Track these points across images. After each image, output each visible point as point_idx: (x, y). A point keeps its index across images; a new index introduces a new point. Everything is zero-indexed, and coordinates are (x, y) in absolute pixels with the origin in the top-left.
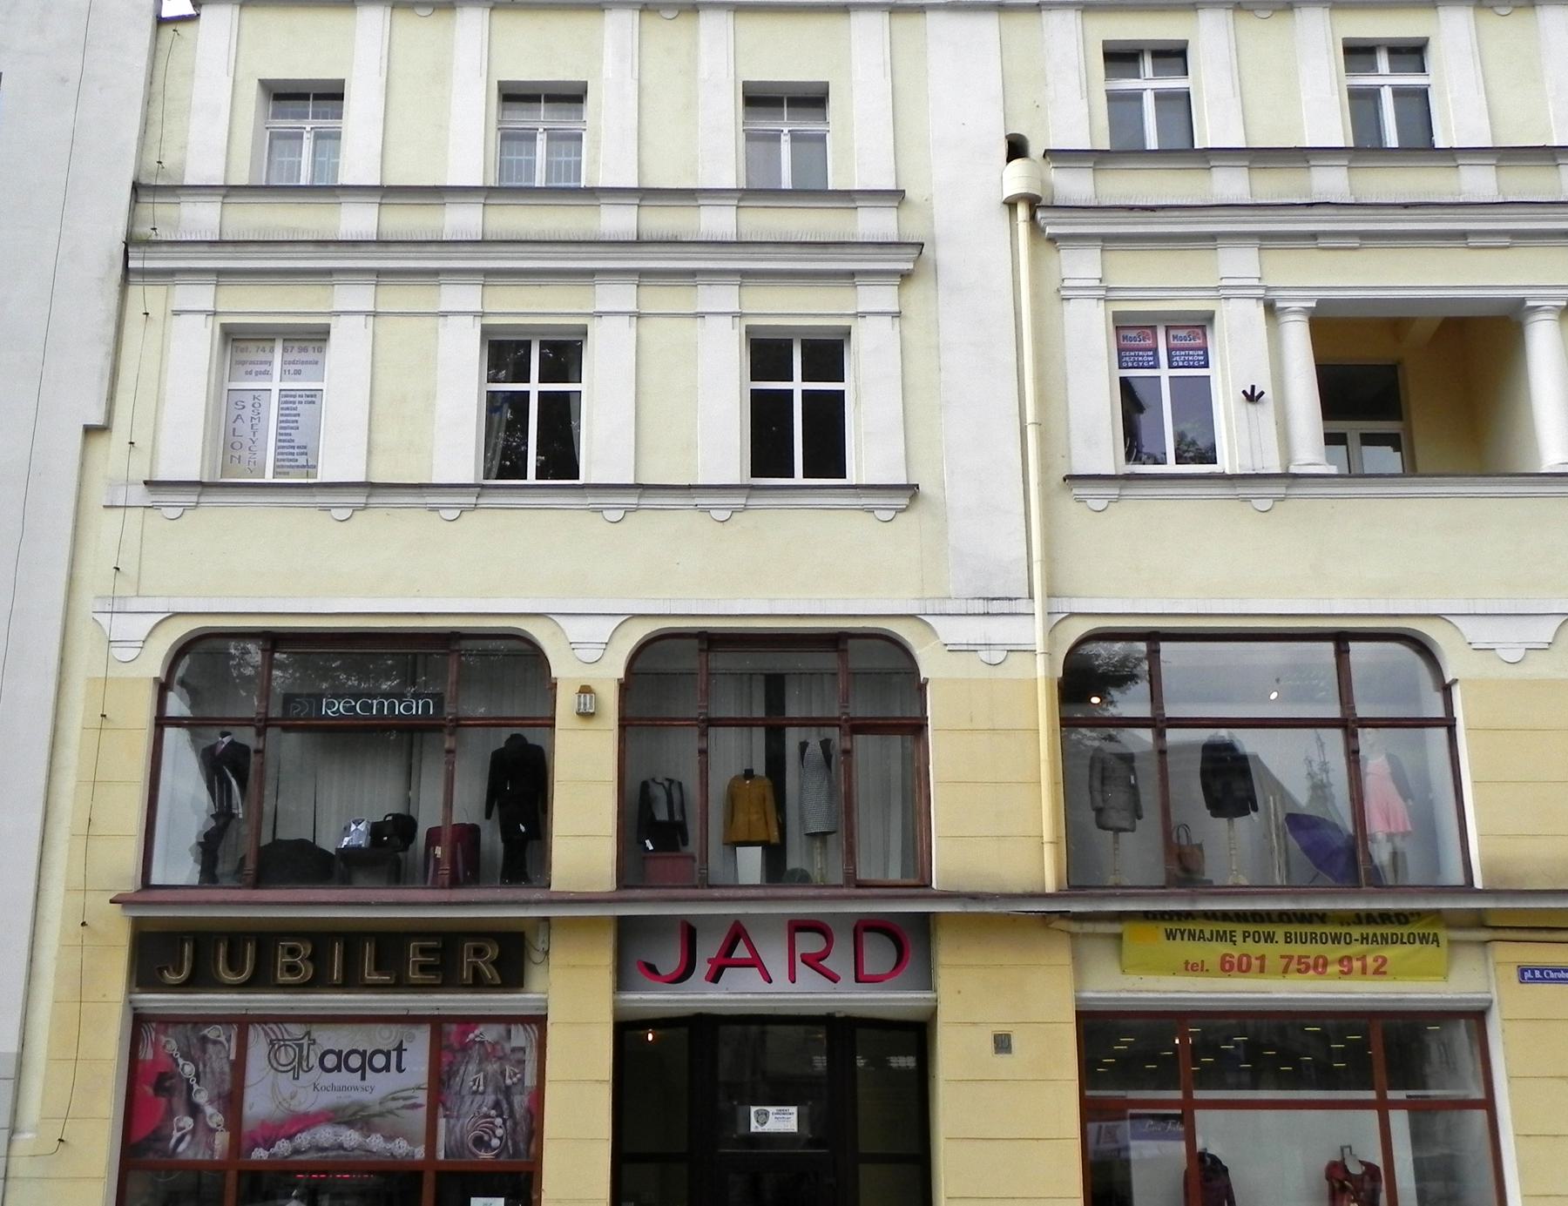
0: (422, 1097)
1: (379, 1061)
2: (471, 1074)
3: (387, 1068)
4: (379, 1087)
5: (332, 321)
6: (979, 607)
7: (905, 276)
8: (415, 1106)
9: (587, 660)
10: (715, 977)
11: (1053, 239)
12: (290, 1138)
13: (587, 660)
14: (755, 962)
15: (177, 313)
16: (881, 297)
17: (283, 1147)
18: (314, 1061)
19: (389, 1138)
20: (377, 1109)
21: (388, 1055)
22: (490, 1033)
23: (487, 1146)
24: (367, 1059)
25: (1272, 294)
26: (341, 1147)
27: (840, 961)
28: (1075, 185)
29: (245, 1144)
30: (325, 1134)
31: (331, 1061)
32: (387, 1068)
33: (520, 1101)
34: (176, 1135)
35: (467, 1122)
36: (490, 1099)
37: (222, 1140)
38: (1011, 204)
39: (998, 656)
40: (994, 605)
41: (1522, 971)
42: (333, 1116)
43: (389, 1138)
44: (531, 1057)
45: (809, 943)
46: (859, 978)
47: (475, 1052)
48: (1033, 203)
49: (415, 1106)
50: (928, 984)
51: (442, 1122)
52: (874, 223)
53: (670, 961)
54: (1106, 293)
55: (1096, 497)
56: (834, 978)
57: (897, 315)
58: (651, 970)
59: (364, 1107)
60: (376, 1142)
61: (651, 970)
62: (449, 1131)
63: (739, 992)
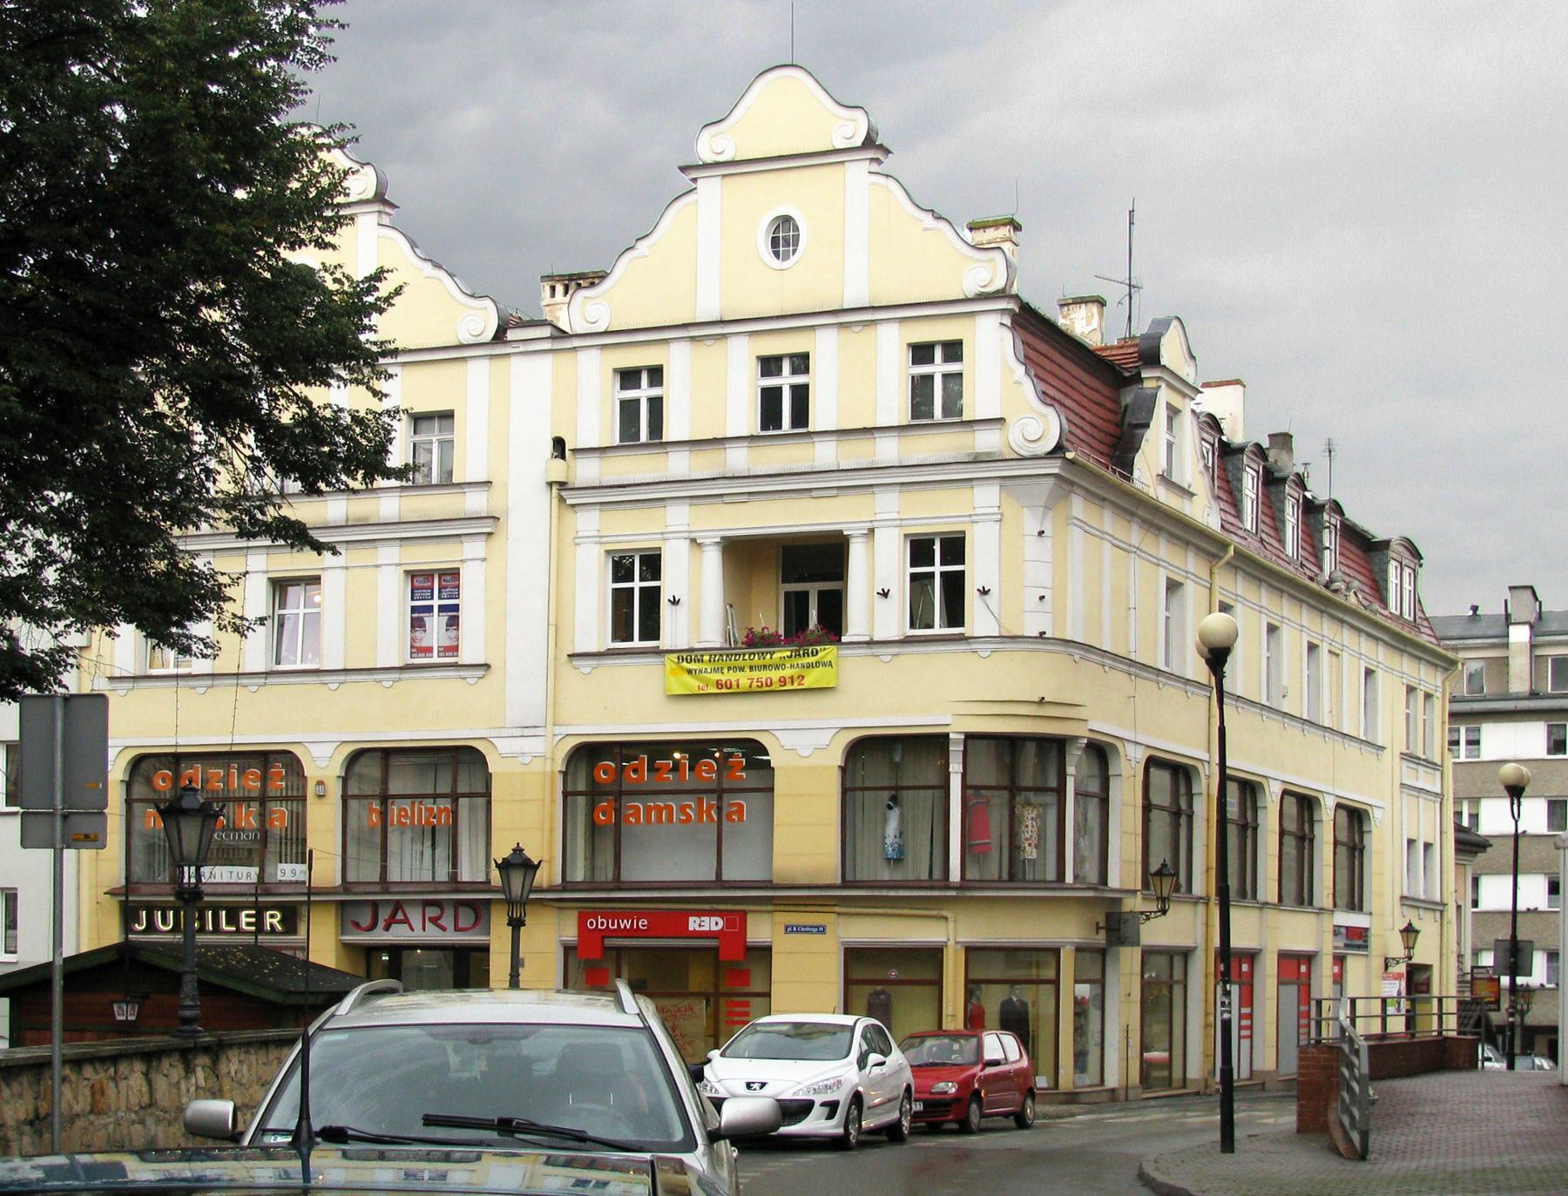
6: (519, 732)
7: (490, 534)
10: (387, 928)
11: (573, 506)
14: (406, 921)
16: (474, 548)
25: (693, 535)
27: (448, 920)
28: (586, 471)
38: (550, 484)
39: (527, 760)
40: (527, 730)
45: (432, 912)
46: (457, 929)
48: (562, 485)
50: (488, 933)
52: (475, 502)
53: (366, 922)
54: (600, 538)
55: (586, 665)
56: (444, 929)
57: (484, 559)
58: (357, 925)
61: (357, 925)
63: (399, 934)
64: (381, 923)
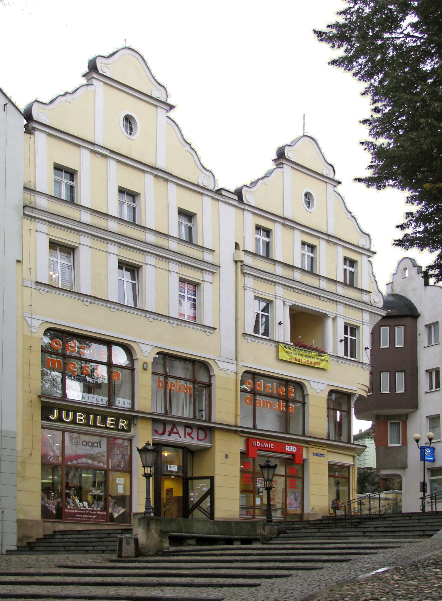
0: (105, 454)
1: (95, 445)
2: (116, 451)
3: (97, 446)
4: (95, 451)
5: (80, 246)
8: (104, 456)
9: (146, 354)
10: (169, 435)
12: (76, 460)
13: (146, 354)
14: (177, 433)
15: (37, 231)
17: (75, 462)
18: (81, 443)
19: (99, 463)
20: (95, 456)
21: (97, 443)
22: (120, 441)
23: (120, 467)
24: (93, 444)
26: (88, 463)
27: (194, 435)
29: (66, 460)
30: (84, 460)
31: (84, 443)
32: (97, 446)
33: (127, 458)
34: (49, 456)
35: (115, 461)
36: (120, 456)
37: (60, 459)
41: (314, 453)
42: (85, 456)
43: (99, 463)
44: (129, 448)
45: (188, 430)
47: (117, 445)
49: (104, 456)
51: (110, 460)
53: (160, 431)
56: (193, 439)
59: (93, 455)
60: (96, 463)
62: (112, 463)
64: (167, 433)
